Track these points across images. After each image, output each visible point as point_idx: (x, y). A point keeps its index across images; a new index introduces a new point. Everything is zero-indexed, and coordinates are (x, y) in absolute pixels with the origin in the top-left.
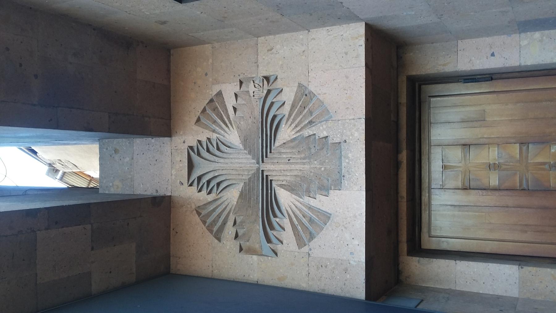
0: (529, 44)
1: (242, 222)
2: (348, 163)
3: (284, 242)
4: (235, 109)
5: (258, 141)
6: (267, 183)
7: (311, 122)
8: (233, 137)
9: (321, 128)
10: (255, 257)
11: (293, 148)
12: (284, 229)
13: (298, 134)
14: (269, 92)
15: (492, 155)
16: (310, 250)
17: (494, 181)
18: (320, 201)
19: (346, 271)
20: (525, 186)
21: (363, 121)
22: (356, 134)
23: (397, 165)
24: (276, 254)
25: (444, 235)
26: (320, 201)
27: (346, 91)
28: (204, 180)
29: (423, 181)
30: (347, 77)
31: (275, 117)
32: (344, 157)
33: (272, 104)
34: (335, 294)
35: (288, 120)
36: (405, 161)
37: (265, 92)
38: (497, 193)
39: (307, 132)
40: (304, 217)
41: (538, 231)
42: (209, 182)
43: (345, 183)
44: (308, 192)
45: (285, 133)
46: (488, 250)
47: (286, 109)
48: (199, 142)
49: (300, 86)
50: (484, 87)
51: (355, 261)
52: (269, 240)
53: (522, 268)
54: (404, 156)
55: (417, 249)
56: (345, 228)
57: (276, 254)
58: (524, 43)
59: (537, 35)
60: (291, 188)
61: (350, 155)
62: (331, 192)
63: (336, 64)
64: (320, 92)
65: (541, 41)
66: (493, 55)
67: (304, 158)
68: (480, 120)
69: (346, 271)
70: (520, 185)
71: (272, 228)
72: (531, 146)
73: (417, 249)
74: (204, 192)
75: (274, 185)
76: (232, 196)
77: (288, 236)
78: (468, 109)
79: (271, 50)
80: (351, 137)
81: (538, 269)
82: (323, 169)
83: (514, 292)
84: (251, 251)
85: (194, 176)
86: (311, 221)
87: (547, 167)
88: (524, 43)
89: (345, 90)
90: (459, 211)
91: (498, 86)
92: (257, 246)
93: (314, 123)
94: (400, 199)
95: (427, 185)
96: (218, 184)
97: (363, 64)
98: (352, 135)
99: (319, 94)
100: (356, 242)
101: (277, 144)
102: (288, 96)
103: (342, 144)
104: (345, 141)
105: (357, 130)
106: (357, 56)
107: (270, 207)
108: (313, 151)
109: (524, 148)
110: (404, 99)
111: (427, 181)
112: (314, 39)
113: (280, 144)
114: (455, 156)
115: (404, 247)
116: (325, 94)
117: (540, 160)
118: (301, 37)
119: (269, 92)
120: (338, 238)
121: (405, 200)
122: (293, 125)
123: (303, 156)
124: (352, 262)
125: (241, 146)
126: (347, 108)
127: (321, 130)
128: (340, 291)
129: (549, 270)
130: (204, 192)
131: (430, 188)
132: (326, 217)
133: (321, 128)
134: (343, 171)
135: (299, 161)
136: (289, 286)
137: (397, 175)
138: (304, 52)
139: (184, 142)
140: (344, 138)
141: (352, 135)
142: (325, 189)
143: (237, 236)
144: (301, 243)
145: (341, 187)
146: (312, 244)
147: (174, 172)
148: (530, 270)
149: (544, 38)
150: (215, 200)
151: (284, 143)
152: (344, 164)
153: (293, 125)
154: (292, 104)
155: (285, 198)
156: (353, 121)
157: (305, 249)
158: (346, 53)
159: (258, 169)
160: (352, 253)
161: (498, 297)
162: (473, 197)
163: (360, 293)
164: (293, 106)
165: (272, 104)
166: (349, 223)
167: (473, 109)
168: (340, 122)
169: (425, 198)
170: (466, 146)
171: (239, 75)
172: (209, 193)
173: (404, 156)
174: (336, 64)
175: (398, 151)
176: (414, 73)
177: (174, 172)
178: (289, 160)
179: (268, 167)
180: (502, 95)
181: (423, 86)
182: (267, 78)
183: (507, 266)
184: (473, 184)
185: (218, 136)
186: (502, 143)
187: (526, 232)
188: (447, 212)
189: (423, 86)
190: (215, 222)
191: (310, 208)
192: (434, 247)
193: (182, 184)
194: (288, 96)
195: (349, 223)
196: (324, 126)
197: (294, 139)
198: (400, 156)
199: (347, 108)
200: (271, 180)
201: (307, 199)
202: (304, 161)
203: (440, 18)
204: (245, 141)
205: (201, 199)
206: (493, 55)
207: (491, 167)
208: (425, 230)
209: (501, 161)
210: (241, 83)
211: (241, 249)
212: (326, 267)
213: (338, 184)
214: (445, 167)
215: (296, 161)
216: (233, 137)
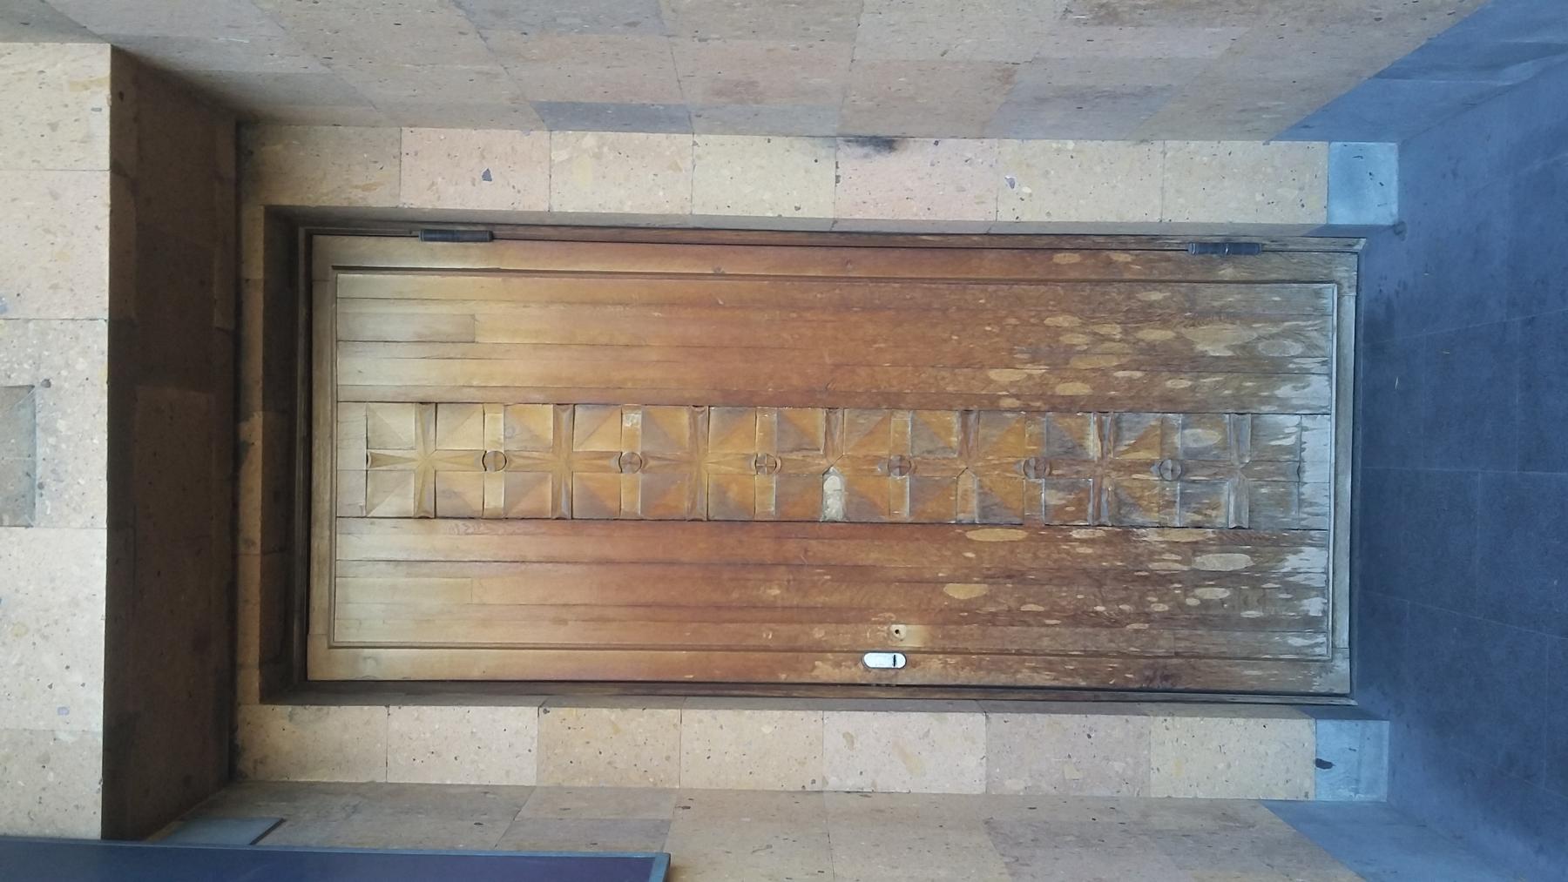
0: (569, 160)
2: (55, 447)
15: (489, 431)
17: (495, 499)
19: (44, 762)
20: (564, 511)
21: (103, 328)
22: (81, 364)
23: (236, 453)
25: (368, 639)
27: (50, 237)
29: (315, 497)
32: (43, 430)
34: (10, 833)
38: (501, 527)
41: (592, 620)
43: (45, 505)
46: (476, 674)
50: (474, 255)
51: (71, 733)
53: (546, 712)
54: (255, 429)
55: (295, 678)
56: (45, 637)
58: (560, 156)
59: (590, 139)
61: (61, 425)
63: (21, 154)
65: (598, 156)
66: (487, 176)
68: (461, 341)
69: (44, 762)
70: (555, 507)
72: (579, 410)
73: (295, 678)
78: (434, 309)
80: (64, 373)
81: (582, 711)
83: (525, 773)
87: (613, 463)
88: (560, 156)
89: (47, 231)
90: (409, 575)
91: (511, 255)
94: (242, 548)
95: (327, 505)
97: (105, 162)
98: (67, 365)
100: (77, 677)
103: (38, 391)
104: (47, 384)
106: (87, 139)
109: (565, 416)
110: (256, 269)
111: (327, 497)
114: (402, 425)
115: (251, 679)
117: (598, 446)
120: (22, 668)
121: (257, 550)
124: (62, 736)
126: (55, 287)
128: (27, 821)
129: (605, 711)
131: (334, 517)
134: (39, 471)
137: (234, 479)
140: (45, 373)
141: (67, 365)
145: (32, 517)
148: (564, 716)
149: (605, 149)
152: (41, 451)
156: (71, 325)
158: (54, 127)
160: (63, 711)
161: (487, 790)
162: (443, 539)
163: (86, 821)
166: (56, 622)
167: (445, 309)
168: (31, 325)
169: (319, 545)
170: (429, 405)
173: (255, 429)
174: (21, 154)
175: (237, 414)
176: (285, 200)
180: (516, 281)
181: (319, 239)
183: (512, 709)
186: (512, 400)
187: (564, 622)
188: (384, 578)
189: (319, 239)
192: (342, 673)
195: (56, 622)
198: (245, 427)
199: (55, 287)
203: (328, 65)
206: (487, 176)
208: (317, 627)
209: (513, 447)
214: (372, 460)
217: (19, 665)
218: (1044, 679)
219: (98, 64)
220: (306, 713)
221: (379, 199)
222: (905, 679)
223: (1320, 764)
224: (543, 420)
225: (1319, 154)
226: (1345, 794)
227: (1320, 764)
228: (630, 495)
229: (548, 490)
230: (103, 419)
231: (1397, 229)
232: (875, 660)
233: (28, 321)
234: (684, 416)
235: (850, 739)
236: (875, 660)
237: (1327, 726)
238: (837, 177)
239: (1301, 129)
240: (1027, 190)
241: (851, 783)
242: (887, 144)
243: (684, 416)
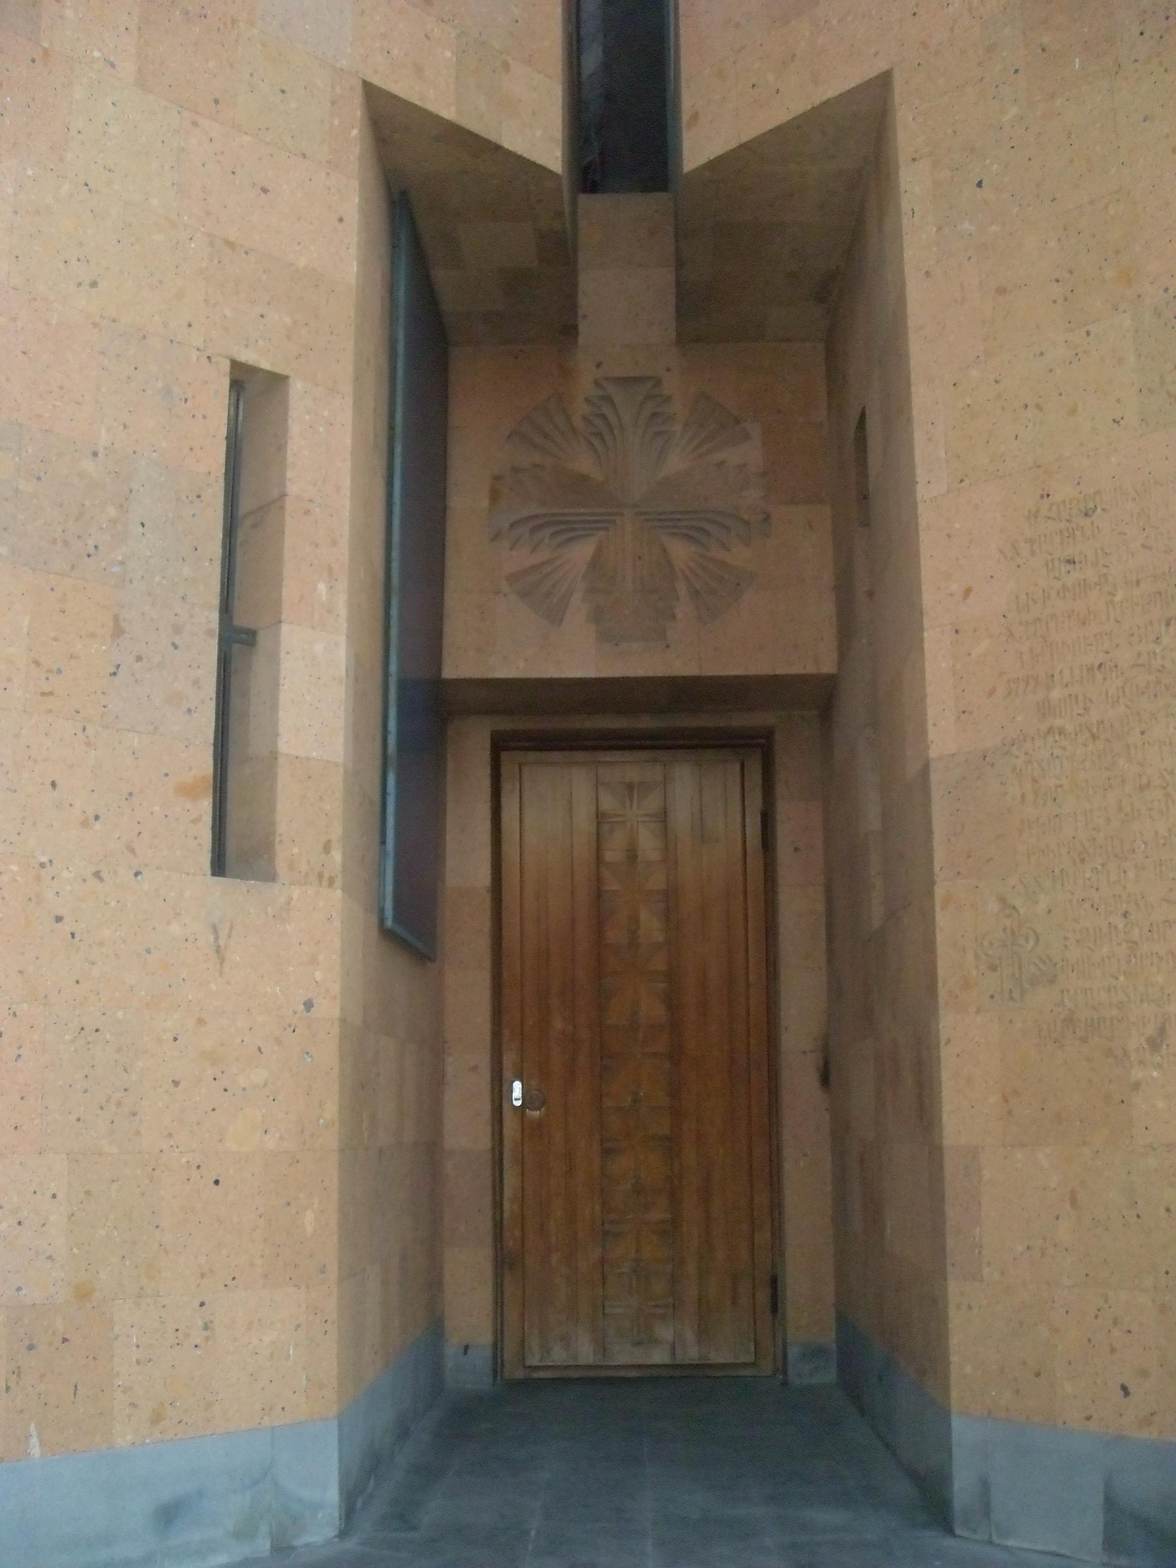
4: (721, 464)
7: (697, 592)
8: (676, 462)
10: (485, 503)
12: (534, 550)
28: (607, 410)
31: (707, 533)
33: (728, 528)
36: (640, 725)
37: (746, 517)
39: (682, 589)
42: (603, 417)
45: (681, 552)
46: (505, 847)
48: (668, 399)
59: (820, 907)
60: (596, 563)
66: (796, 849)
71: (533, 530)
75: (602, 533)
79: (811, 527)
84: (495, 495)
91: (755, 863)
96: (600, 435)
100: (522, 664)
102: (739, 556)
104: (668, 646)
121: (578, 725)
132: (555, 615)
136: (449, 563)
139: (668, 370)
142: (597, 616)
144: (512, 578)
150: (574, 431)
155: (582, 552)
165: (728, 528)
172: (584, 418)
173: (646, 723)
182: (767, 518)
184: (605, 828)
192: (505, 770)
194: (739, 556)
200: (607, 529)
207: (632, 855)
214: (630, 787)
216: (676, 462)
218: (508, 1193)
219: (828, 667)
220: (486, 756)
221: (780, 789)
222: (505, 1106)
223: (466, 1348)
224: (657, 881)
225: (829, 1338)
226: (450, 1364)
227: (466, 1348)
228: (615, 935)
229: (614, 887)
231: (785, 1383)
232: (517, 1087)
234: (661, 967)
235: (474, 1069)
236: (517, 1087)
237: (488, 1353)
238: (804, 1052)
239: (842, 1319)
240: (802, 1164)
241: (450, 1070)
242: (825, 1079)
243: (661, 967)
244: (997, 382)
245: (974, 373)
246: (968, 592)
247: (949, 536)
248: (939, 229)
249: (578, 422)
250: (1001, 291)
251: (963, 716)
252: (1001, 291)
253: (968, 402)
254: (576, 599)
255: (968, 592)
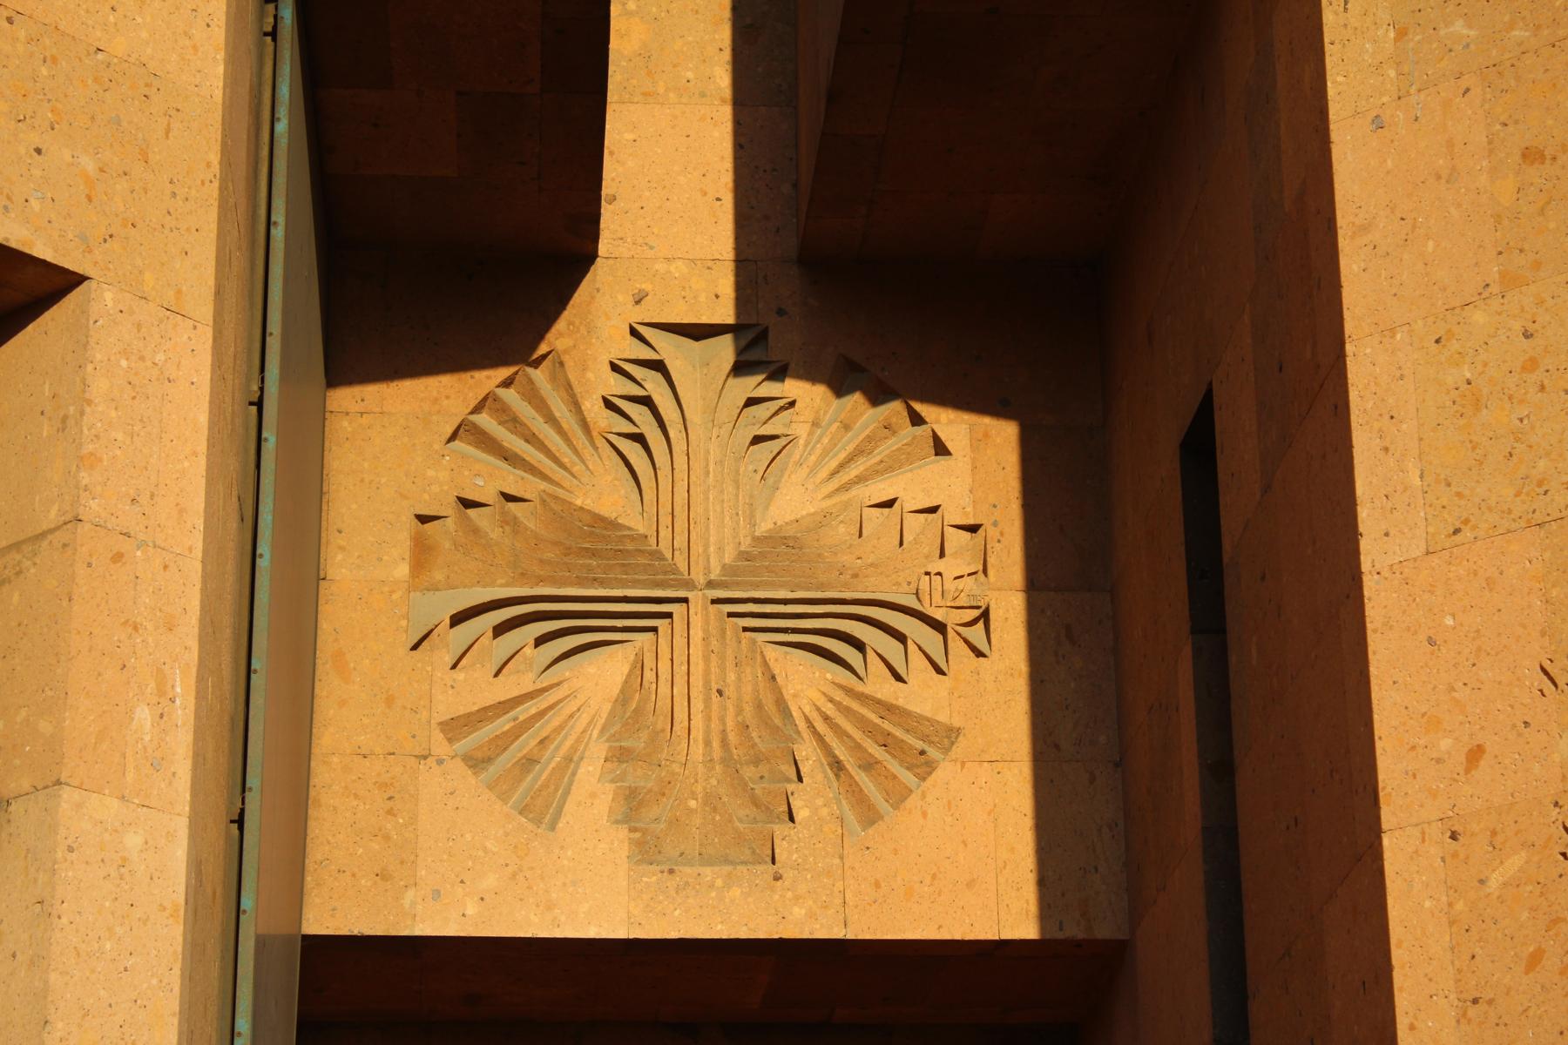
1: (513, 524)
2: (712, 886)
3: (459, 675)
5: (782, 586)
6: (648, 615)
7: (837, 766)
8: (795, 500)
9: (820, 802)
10: (403, 570)
11: (759, 707)
13: (802, 725)
14: (940, 627)
16: (440, 762)
18: (593, 795)
22: (798, 912)
24: (415, 647)
26: (593, 795)
27: (928, 880)
28: (653, 384)
30: (970, 884)
32: (730, 874)
35: (849, 691)
37: (939, 615)
39: (807, 752)
40: (542, 742)
42: (646, 401)
44: (620, 755)
45: (806, 682)
47: (879, 685)
49: (951, 734)
51: (413, 904)
52: (458, 619)
56: (514, 876)
57: (415, 647)
60: (631, 706)
61: (736, 892)
62: (623, 832)
63: (1012, 850)
64: (929, 799)
67: (724, 743)
69: (383, 875)
71: (500, 630)
74: (617, 386)
76: (602, 490)
77: (477, 687)
80: (789, 894)
82: (693, 804)
84: (422, 555)
85: (668, 348)
86: (528, 763)
89: (934, 876)
92: (439, 576)
93: (837, 776)
96: (639, 438)
98: (797, 898)
99: (924, 796)
101: (773, 653)
104: (777, 878)
105: (811, 915)
107: (571, 624)
108: (749, 772)
112: (1092, 779)
113: (772, 663)
116: (924, 815)
118: (1102, 739)
119: (940, 627)
120: (481, 853)
122: (829, 709)
123: (732, 738)
125: (764, 527)
126: (877, 885)
127: (815, 799)
128: (319, 857)
130: (617, 386)
132: (543, 810)
133: (820, 802)
134: (688, 870)
135: (715, 725)
138: (1057, 746)
140: (789, 875)
141: (797, 898)
142: (632, 806)
143: (467, 504)
144: (455, 727)
145: (639, 862)
146: (459, 767)
147: (679, 268)
150: (585, 426)
151: (773, 677)
152: (708, 872)
153: (829, 709)
154: (898, 708)
155: (601, 675)
156: (838, 901)
157: (440, 745)
159: (689, 585)
160: (437, 894)
163: (318, 922)
164: (889, 709)
165: (901, 638)
166: (529, 888)
168: (837, 861)
171: (995, 524)
177: (679, 268)
178: (720, 692)
179: (700, 618)
185: (802, 442)
190: (513, 422)
191: (571, 761)
193: (638, 302)
194: (923, 695)
195: (529, 888)
196: (824, 812)
197: (785, 712)
199: (877, 885)
200: (654, 630)
201: (598, 750)
202: (716, 744)
204: (780, 545)
205: (590, 375)
210: (973, 529)
211: (424, 519)
212: (390, 812)
213: (646, 850)
215: (714, 716)
217: (486, 850)
230: (743, 934)
233: (842, 858)
244: (1527, 335)
245: (1479, 317)
246: (1475, 754)
247: (1431, 642)
248: (1401, 34)
249: (593, 409)
250: (1532, 155)
251: (1473, 1011)
252: (1532, 155)
253: (1468, 375)
254: (590, 771)
255: (1475, 754)
